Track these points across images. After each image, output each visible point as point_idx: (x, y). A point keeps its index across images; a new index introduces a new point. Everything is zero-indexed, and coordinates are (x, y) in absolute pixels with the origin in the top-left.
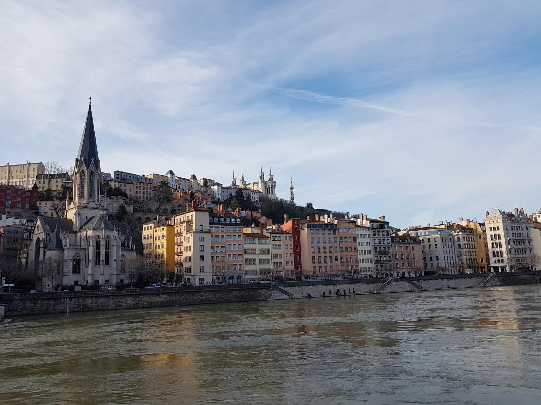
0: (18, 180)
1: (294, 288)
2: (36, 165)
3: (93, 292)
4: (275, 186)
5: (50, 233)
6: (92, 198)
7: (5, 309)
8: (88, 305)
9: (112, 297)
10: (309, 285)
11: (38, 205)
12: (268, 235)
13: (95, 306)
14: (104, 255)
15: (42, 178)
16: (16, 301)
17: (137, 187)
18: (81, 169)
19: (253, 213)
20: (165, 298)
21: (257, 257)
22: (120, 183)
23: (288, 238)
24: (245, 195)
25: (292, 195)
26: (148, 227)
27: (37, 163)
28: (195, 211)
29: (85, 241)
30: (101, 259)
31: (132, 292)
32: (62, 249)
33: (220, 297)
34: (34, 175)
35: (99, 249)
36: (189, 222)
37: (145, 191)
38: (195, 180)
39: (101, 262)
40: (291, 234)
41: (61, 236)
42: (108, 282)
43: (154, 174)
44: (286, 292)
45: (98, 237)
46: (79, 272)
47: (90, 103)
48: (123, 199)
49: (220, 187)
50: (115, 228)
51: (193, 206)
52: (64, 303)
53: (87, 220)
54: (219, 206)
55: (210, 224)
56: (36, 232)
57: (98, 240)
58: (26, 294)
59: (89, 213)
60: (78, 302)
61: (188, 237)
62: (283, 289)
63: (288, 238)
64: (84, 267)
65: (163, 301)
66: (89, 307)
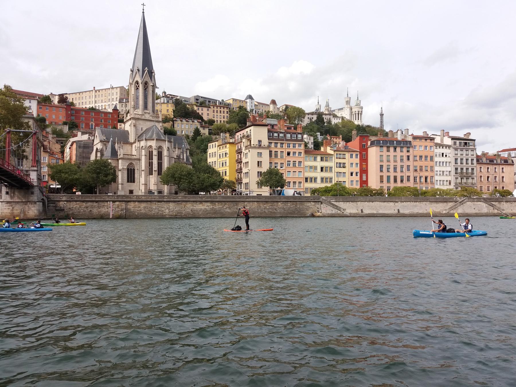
0: (103, 104)
1: (348, 203)
2: (119, 89)
3: (135, 197)
4: (361, 112)
5: (107, 143)
8: (130, 209)
10: (365, 201)
12: (332, 152)
13: (138, 211)
15: (124, 101)
17: (214, 111)
18: (136, 80)
20: (208, 206)
21: (319, 175)
23: (354, 156)
24: (325, 120)
25: (382, 122)
26: (213, 145)
30: (154, 169)
34: (117, 98)
35: (152, 159)
37: (222, 114)
38: (275, 106)
39: (154, 172)
40: (358, 151)
41: (116, 146)
44: (337, 206)
46: (134, 182)
47: (143, 9)
52: (107, 206)
53: (143, 131)
55: (269, 139)
58: (72, 196)
60: (121, 206)
62: (336, 204)
63: (354, 156)
64: (139, 177)
65: (205, 209)
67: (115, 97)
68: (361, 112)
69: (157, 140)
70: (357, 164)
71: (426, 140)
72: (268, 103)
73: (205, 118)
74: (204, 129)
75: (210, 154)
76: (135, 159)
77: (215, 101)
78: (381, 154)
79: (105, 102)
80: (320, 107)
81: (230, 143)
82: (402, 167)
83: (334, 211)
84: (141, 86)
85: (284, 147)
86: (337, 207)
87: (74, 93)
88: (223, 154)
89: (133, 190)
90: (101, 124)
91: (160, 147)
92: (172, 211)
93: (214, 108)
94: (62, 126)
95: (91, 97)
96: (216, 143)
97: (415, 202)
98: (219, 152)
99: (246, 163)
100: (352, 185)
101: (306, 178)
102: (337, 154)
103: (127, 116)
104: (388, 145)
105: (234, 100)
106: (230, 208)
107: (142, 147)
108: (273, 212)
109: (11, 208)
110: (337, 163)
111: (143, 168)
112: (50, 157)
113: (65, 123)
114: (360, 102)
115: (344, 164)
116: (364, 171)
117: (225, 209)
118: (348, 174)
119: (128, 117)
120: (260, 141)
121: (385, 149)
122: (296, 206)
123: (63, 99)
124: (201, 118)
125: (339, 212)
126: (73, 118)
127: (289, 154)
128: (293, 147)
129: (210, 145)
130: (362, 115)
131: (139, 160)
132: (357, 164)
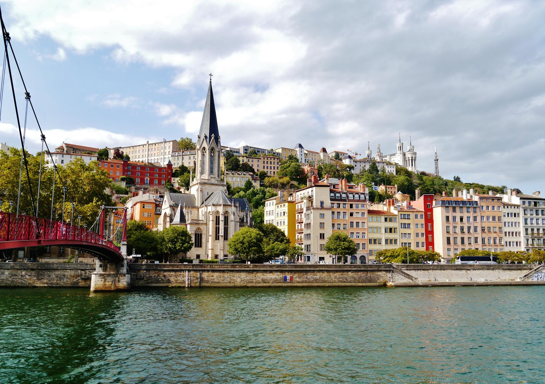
2: (171, 143)
3: (209, 266)
6: (213, 174)
7: (131, 277)
8: (204, 278)
10: (437, 269)
11: (172, 181)
12: (396, 212)
14: (223, 231)
19: (387, 188)
22: (248, 159)
23: (419, 216)
24: (379, 168)
25: (437, 168)
26: (270, 203)
27: (172, 141)
28: (316, 186)
31: (245, 268)
32: (185, 224)
33: (335, 277)
34: (169, 152)
35: (219, 224)
36: (310, 198)
37: (272, 165)
38: (325, 154)
39: (220, 237)
40: (422, 212)
41: (184, 210)
42: (227, 257)
43: (282, 148)
46: (201, 246)
47: (211, 79)
48: (250, 175)
49: (352, 161)
50: (233, 204)
51: (313, 181)
52: (183, 275)
53: (209, 196)
54: (342, 181)
55: (331, 200)
56: (163, 207)
57: (218, 216)
59: (209, 189)
61: (308, 214)
62: (406, 272)
66: (206, 280)
67: (167, 151)
68: (415, 158)
69: (224, 205)
70: (422, 225)
71: (493, 200)
72: (319, 150)
76: (202, 224)
77: (263, 151)
78: (448, 214)
79: (158, 156)
80: (371, 152)
81: (289, 202)
82: (469, 228)
83: (406, 281)
85: (346, 208)
86: (408, 276)
87: (128, 147)
90: (155, 178)
91: (226, 212)
92: (243, 280)
93: (264, 159)
94: (120, 182)
95: (145, 150)
97: (487, 269)
98: (276, 210)
99: (307, 224)
100: (418, 246)
101: (370, 240)
102: (401, 214)
103: (193, 180)
104: (454, 205)
105: (283, 149)
106: (299, 277)
107: (210, 212)
108: (344, 281)
109: (103, 279)
110: (402, 224)
111: (210, 233)
112: (115, 217)
113: (123, 179)
114: (413, 148)
115: (409, 224)
116: (429, 233)
117: (295, 278)
118: (413, 236)
120: (322, 203)
121: (451, 209)
122: (367, 275)
123: (119, 154)
124: (253, 171)
125: (411, 281)
126: (129, 173)
127: (351, 214)
128: (356, 207)
129: (267, 203)
130: (416, 161)
131: (206, 224)
132: (422, 225)
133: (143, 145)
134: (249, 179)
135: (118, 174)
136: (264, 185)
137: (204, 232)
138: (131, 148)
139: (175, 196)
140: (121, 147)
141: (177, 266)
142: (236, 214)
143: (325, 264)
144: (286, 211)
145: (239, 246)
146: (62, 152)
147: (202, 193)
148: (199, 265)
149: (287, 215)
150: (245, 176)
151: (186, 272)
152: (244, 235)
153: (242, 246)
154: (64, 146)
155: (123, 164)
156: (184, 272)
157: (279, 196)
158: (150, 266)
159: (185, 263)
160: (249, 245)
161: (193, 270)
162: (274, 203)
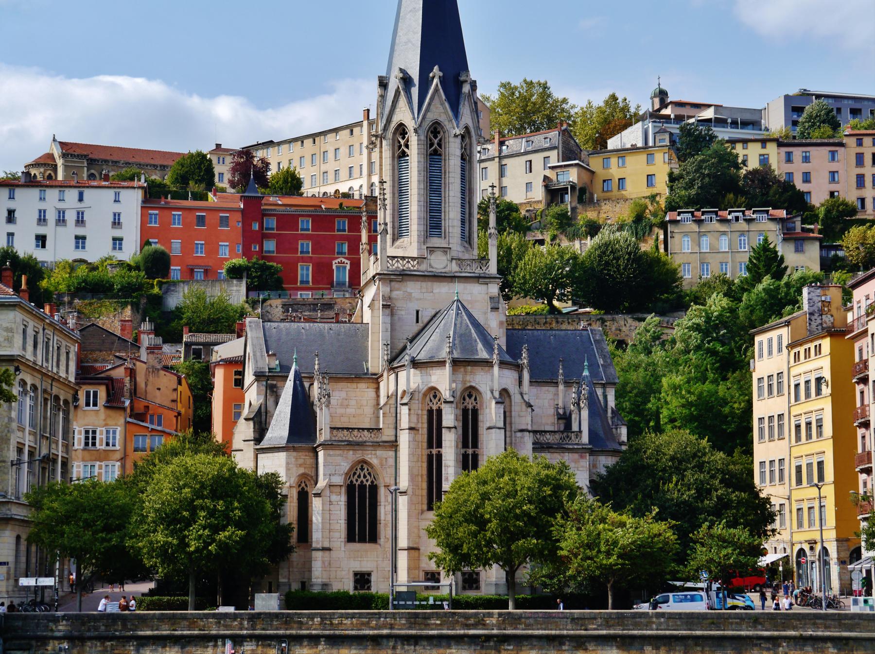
3: (317, 620)
5: (279, 384)
6: (440, 236)
9: (391, 644)
16: (56, 642)
22: (784, 150)
26: (770, 341)
29: (393, 410)
45: (435, 397)
46: (373, 538)
48: (773, 219)
53: (421, 325)
57: (434, 408)
69: (456, 363)
73: (818, 198)
74: (798, 250)
75: (760, 380)
84: (413, 140)
87: (295, 140)
88: (807, 382)
89: (369, 574)
91: (471, 392)
93: (860, 143)
94: (225, 286)
96: (784, 332)
98: (794, 372)
111: (404, 482)
113: (235, 273)
119: (371, 273)
126: (270, 246)
129: (761, 343)
131: (394, 445)
133: (350, 128)
134: (766, 240)
135: (224, 251)
136: (843, 259)
137: (384, 478)
138: (308, 142)
139: (288, 334)
140: (270, 144)
141: (192, 622)
142: (516, 398)
143: (867, 611)
144: (827, 374)
145: (461, 532)
146: (50, 177)
147: (392, 314)
148: (276, 616)
149: (829, 391)
150: (754, 227)
151: (224, 645)
152: (489, 488)
153: (475, 535)
154: (57, 152)
155: (243, 212)
156: (215, 646)
157: (806, 307)
158: (83, 624)
159: (223, 610)
160: (505, 530)
161: (251, 637)
162: (785, 343)
